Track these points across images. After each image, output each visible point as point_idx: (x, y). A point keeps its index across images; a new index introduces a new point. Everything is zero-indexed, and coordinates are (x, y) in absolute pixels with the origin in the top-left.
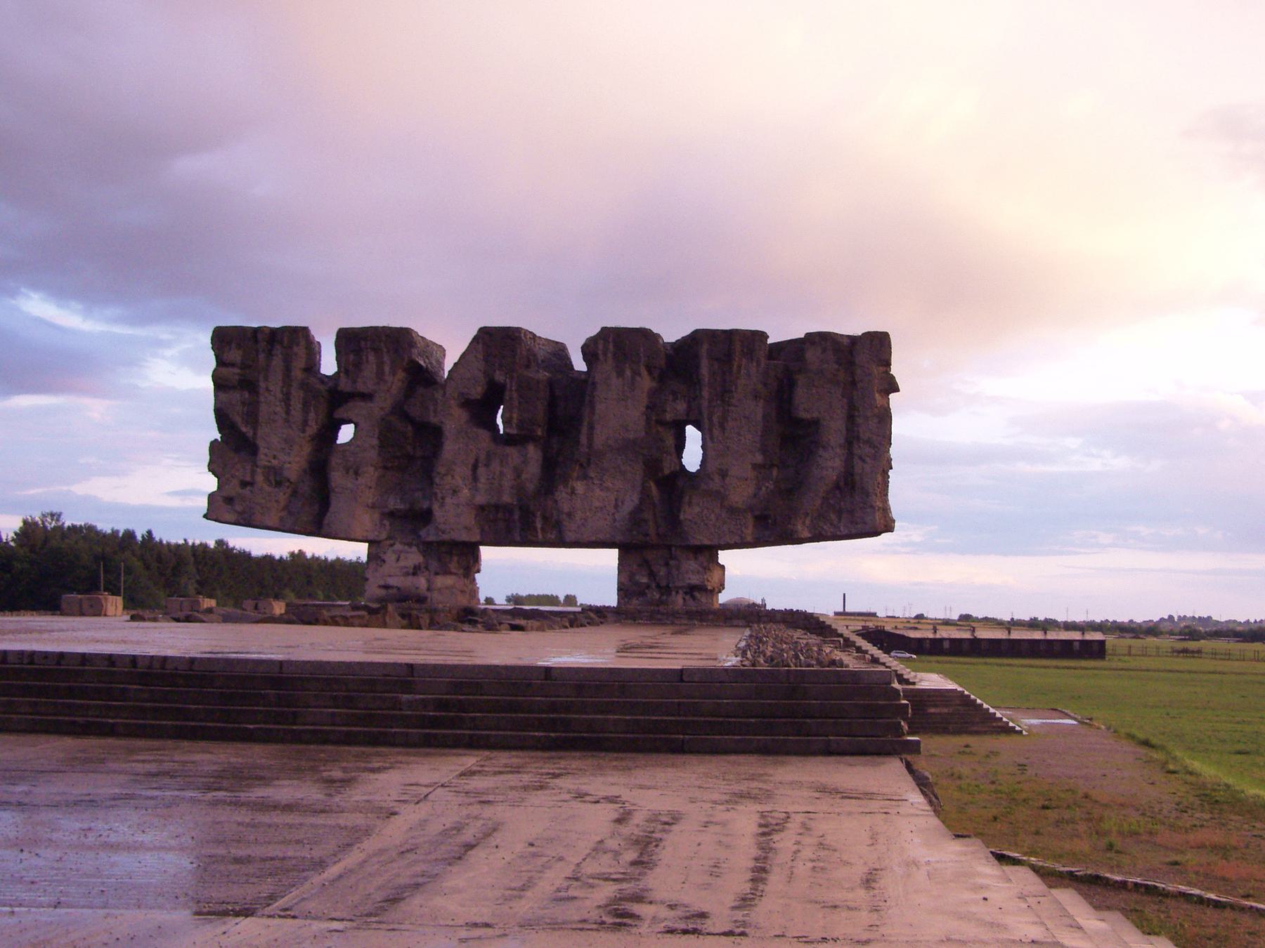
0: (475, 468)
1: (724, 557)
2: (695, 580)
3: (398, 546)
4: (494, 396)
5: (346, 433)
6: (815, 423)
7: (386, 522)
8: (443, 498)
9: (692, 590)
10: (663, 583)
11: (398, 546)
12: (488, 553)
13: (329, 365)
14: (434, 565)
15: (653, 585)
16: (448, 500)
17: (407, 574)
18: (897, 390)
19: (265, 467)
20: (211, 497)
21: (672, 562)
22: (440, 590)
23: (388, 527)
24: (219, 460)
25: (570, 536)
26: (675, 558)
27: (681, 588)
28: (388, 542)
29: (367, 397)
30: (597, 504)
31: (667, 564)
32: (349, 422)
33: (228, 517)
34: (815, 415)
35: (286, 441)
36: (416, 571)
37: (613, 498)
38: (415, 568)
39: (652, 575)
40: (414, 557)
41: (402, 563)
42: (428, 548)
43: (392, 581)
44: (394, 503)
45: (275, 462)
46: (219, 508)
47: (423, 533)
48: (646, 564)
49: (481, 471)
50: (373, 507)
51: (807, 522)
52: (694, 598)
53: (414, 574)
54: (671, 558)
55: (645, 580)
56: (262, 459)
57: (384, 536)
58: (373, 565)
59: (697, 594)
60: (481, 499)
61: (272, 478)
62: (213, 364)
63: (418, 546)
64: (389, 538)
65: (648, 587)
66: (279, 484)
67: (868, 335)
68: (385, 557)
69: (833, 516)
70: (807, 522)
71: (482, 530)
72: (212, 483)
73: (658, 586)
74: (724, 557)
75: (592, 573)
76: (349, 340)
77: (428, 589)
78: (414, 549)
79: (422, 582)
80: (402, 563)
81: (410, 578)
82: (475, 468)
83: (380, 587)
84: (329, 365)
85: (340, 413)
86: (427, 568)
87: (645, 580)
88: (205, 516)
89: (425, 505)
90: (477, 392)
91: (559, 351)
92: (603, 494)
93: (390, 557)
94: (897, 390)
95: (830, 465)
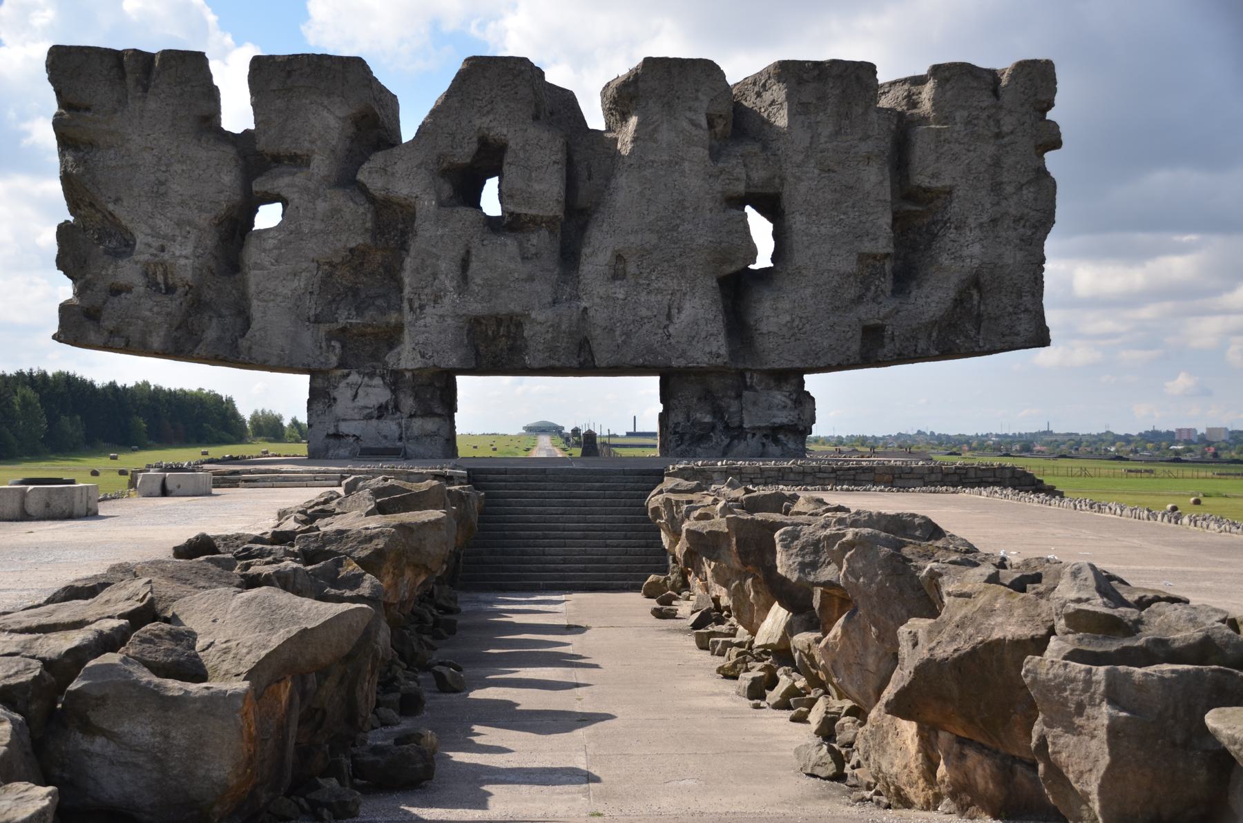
0: (465, 264)
1: (813, 383)
2: (782, 418)
3: (354, 378)
4: (490, 158)
5: (268, 216)
6: (949, 192)
7: (333, 343)
8: (422, 307)
9: (773, 433)
10: (735, 422)
11: (354, 378)
12: (465, 385)
13: (237, 114)
14: (408, 403)
15: (720, 426)
16: (428, 310)
17: (369, 417)
18: (1056, 144)
19: (147, 264)
20: (64, 309)
21: (745, 393)
22: (417, 438)
23: (338, 351)
24: (73, 252)
25: (601, 359)
26: (751, 388)
27: (759, 428)
28: (339, 372)
29: (298, 161)
30: (644, 312)
31: (739, 396)
32: (270, 199)
33: (92, 336)
34: (948, 182)
35: (179, 224)
36: (382, 411)
37: (665, 302)
38: (380, 407)
39: (718, 412)
40: (378, 394)
41: (361, 401)
42: (395, 380)
43: (344, 428)
44: (344, 317)
45: (166, 256)
46: (77, 326)
47: (390, 359)
48: (708, 396)
49: (474, 265)
50: (317, 320)
51: (934, 334)
52: (776, 441)
53: (379, 417)
54: (747, 388)
55: (708, 419)
56: (142, 254)
57: (334, 360)
58: (319, 406)
59: (781, 436)
60: (476, 307)
61: (160, 278)
62: (53, 106)
63: (383, 377)
64: (342, 365)
65: (713, 427)
66: (170, 290)
67: (1024, 67)
68: (335, 394)
69: (968, 326)
70: (934, 334)
71: (477, 353)
72: (65, 289)
73: (727, 427)
74: (813, 383)
75: (626, 406)
76: (267, 74)
77: (400, 439)
78: (377, 381)
79: (390, 426)
80: (361, 401)
81: (374, 422)
82: (465, 264)
83: (328, 436)
84: (237, 114)
85: (258, 186)
86: (397, 408)
87: (708, 419)
88: (54, 337)
89: (393, 318)
90: (464, 153)
91: (566, 101)
92: (653, 298)
93: (343, 394)
94: (1056, 144)
95: (964, 251)
